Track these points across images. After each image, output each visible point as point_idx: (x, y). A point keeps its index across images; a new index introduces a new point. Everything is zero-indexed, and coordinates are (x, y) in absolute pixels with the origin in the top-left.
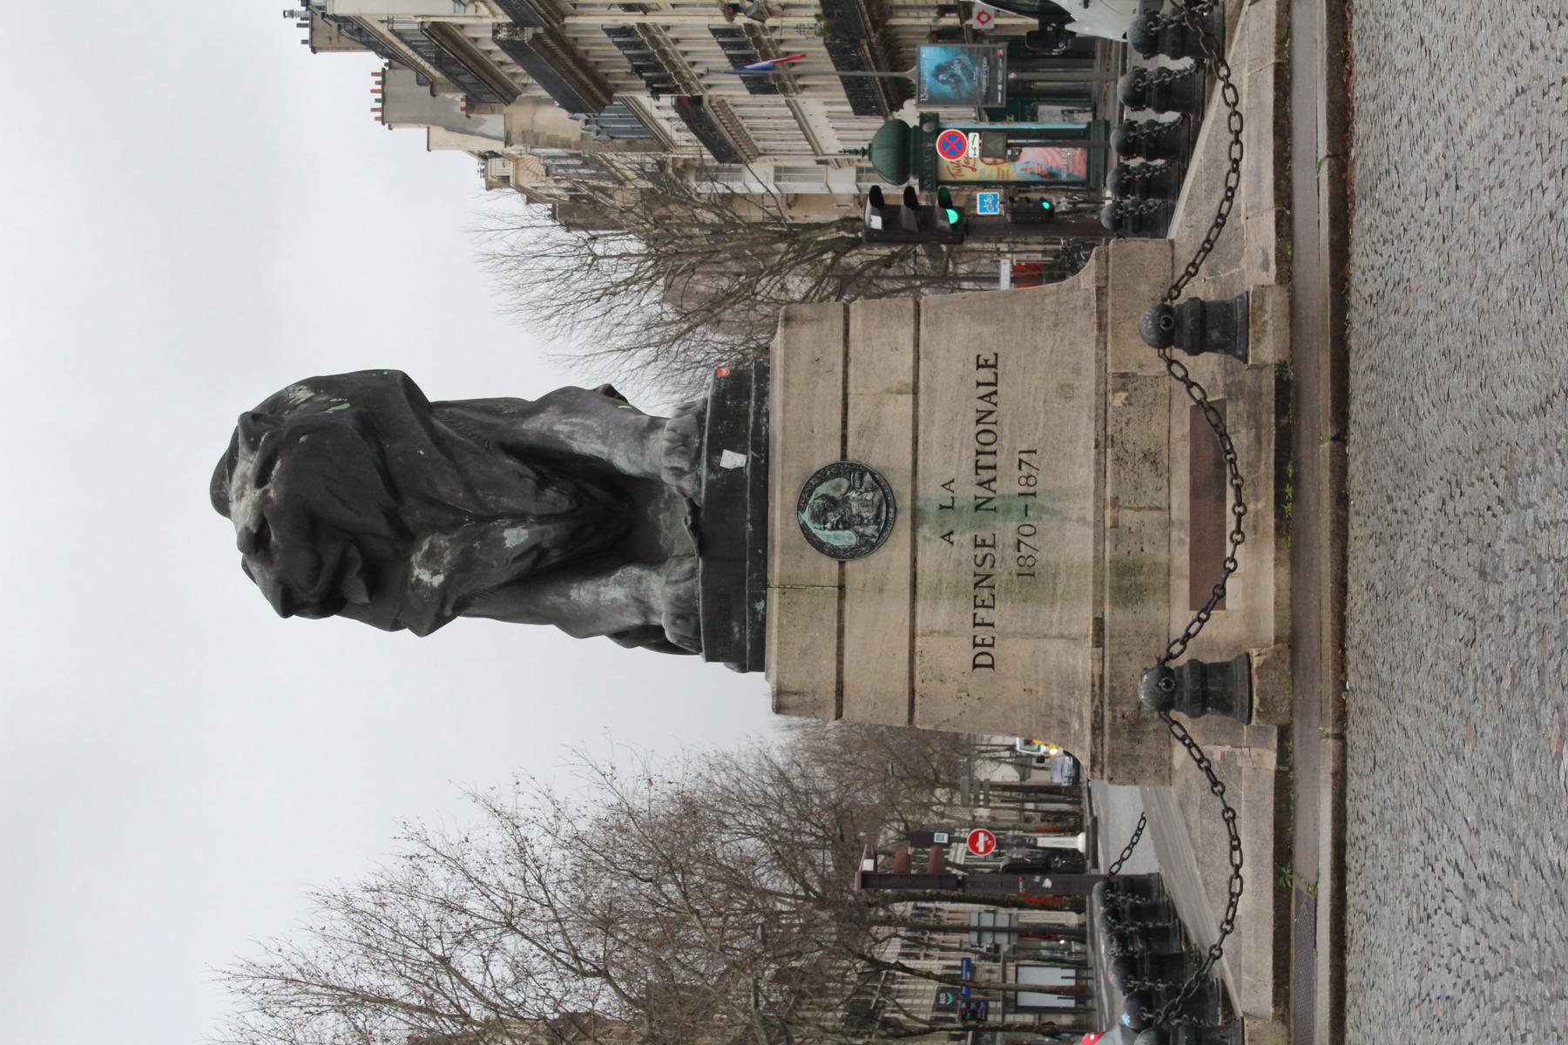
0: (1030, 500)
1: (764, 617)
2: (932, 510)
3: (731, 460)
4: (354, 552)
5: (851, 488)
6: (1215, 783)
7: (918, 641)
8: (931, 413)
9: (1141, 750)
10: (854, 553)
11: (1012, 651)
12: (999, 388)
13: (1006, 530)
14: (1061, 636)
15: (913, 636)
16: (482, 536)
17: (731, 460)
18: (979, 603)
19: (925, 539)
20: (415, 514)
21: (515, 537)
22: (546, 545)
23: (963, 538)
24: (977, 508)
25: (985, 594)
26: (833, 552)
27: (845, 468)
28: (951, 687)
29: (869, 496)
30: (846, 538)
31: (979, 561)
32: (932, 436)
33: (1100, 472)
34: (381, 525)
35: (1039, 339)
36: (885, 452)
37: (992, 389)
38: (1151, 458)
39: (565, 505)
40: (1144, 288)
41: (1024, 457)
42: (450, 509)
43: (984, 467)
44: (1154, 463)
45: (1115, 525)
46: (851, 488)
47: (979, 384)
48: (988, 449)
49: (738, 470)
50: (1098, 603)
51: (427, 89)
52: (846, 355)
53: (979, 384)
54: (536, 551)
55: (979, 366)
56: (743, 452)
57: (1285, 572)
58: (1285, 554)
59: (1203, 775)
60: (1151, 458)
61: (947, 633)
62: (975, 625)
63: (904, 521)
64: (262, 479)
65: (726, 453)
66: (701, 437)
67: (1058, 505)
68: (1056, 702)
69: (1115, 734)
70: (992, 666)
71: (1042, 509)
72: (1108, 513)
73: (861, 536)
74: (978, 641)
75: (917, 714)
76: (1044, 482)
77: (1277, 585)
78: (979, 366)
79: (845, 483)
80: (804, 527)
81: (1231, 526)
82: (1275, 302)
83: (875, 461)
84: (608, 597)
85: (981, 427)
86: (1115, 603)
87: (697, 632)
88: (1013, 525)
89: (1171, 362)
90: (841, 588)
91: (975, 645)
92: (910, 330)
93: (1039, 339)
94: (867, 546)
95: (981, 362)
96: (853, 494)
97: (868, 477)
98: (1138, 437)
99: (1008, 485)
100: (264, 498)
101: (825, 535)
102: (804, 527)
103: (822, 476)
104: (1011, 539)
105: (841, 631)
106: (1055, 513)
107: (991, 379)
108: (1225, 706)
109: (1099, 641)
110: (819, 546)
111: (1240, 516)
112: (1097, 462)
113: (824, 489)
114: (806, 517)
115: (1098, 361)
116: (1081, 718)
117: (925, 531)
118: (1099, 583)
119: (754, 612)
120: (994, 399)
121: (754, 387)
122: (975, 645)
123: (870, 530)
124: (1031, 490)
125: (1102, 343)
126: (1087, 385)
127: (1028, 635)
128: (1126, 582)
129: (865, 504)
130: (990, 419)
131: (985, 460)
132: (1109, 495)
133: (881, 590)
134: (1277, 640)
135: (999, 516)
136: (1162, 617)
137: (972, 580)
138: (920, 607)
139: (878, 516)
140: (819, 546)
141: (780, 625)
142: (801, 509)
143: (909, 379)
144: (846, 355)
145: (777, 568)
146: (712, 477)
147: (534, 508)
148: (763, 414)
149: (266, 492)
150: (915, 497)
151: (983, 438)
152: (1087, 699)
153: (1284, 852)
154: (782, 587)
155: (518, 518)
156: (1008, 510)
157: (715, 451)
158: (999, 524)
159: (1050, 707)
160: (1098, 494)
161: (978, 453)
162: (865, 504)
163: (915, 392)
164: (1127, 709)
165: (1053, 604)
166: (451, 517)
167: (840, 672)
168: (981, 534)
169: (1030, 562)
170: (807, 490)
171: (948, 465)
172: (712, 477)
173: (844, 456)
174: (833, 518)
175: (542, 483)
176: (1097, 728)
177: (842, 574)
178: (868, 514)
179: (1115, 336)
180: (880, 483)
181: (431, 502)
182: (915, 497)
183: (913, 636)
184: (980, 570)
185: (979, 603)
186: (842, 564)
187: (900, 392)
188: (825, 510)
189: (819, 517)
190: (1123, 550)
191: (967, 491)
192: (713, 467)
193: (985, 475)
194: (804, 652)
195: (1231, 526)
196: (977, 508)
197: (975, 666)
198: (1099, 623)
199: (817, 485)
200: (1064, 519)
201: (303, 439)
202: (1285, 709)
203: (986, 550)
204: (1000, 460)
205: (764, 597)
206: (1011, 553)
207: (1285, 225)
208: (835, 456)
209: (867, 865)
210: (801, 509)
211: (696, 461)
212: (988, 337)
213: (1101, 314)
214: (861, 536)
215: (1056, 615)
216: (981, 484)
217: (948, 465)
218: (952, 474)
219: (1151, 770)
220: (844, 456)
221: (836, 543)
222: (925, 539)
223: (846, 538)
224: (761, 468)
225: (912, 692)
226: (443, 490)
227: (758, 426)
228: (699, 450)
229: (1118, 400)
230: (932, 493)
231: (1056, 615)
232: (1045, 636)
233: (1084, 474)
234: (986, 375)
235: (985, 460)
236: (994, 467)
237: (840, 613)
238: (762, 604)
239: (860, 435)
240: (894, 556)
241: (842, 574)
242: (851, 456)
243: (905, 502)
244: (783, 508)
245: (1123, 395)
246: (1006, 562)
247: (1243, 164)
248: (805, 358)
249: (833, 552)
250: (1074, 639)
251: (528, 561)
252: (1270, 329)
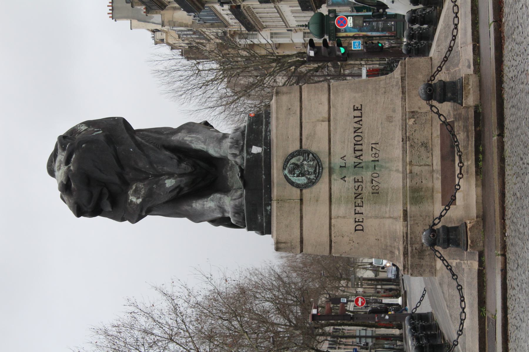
0: (376, 163)
1: (271, 212)
2: (337, 168)
3: (256, 150)
4: (105, 191)
5: (304, 160)
6: (454, 275)
7: (333, 221)
8: (336, 129)
9: (423, 262)
11: (370, 224)
12: (363, 118)
13: (367, 175)
14: (390, 217)
15: (330, 219)
16: (157, 183)
17: (256, 150)
18: (357, 205)
19: (335, 180)
20: (130, 175)
21: (170, 183)
22: (182, 186)
23: (350, 179)
24: (355, 167)
25: (359, 201)
26: (298, 186)
27: (301, 152)
28: (346, 239)
29: (311, 163)
30: (302, 180)
31: (356, 188)
32: (336, 138)
33: (404, 151)
34: (116, 180)
35: (379, 98)
36: (318, 145)
37: (360, 119)
38: (424, 145)
39: (189, 169)
40: (420, 77)
41: (374, 146)
42: (145, 172)
43: (357, 150)
44: (426, 147)
45: (411, 172)
46: (304, 160)
47: (355, 117)
48: (359, 143)
49: (259, 154)
50: (405, 204)
51: (130, 5)
52: (301, 107)
53: (355, 117)
54: (178, 188)
55: (354, 110)
56: (261, 146)
57: (480, 189)
58: (480, 182)
59: (449, 272)
60: (424, 145)
61: (344, 217)
62: (355, 214)
63: (326, 173)
64: (67, 162)
65: (254, 147)
66: (244, 141)
67: (388, 165)
68: (389, 244)
69: (413, 256)
70: (362, 230)
71: (381, 167)
72: (408, 167)
73: (309, 179)
74: (357, 220)
75: (333, 250)
76: (382, 156)
77: (477, 195)
78: (354, 110)
79: (302, 158)
80: (286, 176)
81: (457, 171)
82: (473, 81)
83: (314, 149)
84: (208, 206)
85: (356, 134)
86: (411, 204)
87: (244, 219)
88: (370, 173)
89: (432, 106)
90: (301, 200)
91: (356, 222)
92: (326, 96)
93: (379, 98)
94: (311, 183)
95: (355, 108)
96: (305, 162)
97: (311, 155)
98: (420, 136)
99: (368, 157)
100: (69, 170)
101: (294, 179)
102: (286, 176)
103: (292, 155)
104: (369, 179)
105: (301, 218)
106: (386, 168)
107: (360, 115)
108: (457, 244)
109: (405, 219)
110: (292, 183)
111: (461, 167)
112: (403, 147)
113: (293, 161)
114: (286, 172)
115: (402, 107)
116: (399, 249)
117: (334, 176)
118: (405, 196)
119: (266, 210)
120: (361, 123)
121: (264, 120)
122: (356, 222)
123: (312, 177)
124: (377, 159)
125: (404, 99)
126: (398, 116)
127: (376, 217)
128: (416, 195)
129: (310, 166)
130: (360, 131)
131: (358, 147)
132: (408, 160)
133: (317, 201)
134: (477, 217)
135: (364, 170)
136: (431, 209)
137: (354, 196)
138: (333, 207)
139: (315, 171)
140: (292, 183)
141: (277, 216)
142: (284, 169)
143: (326, 116)
144: (301, 107)
145: (275, 193)
146: (248, 157)
147: (178, 171)
148: (268, 131)
149: (69, 167)
150: (330, 163)
151: (357, 139)
152: (401, 243)
153: (482, 302)
154: (278, 200)
155: (171, 175)
156: (367, 167)
157: (249, 146)
158: (364, 173)
159: (386, 246)
160: (404, 160)
161: (355, 145)
162: (310, 166)
163: (329, 121)
164: (417, 246)
165: (386, 205)
166: (144, 175)
167: (301, 234)
168: (357, 177)
169: (377, 188)
170: (287, 161)
171: (343, 150)
172: (248, 157)
173: (301, 147)
174: (297, 172)
175: (180, 161)
176: (405, 254)
177: (301, 195)
178: (311, 170)
179: (409, 96)
180: (316, 158)
181: (136, 169)
182: (330, 163)
183: (330, 219)
184: (356, 192)
185: (357, 205)
186: (301, 190)
187: (323, 121)
188: (294, 169)
189: (292, 172)
190: (414, 182)
191: (351, 160)
192: (249, 153)
193: (358, 153)
194: (287, 226)
195: (457, 171)
196: (355, 167)
197: (356, 230)
198: (405, 212)
199: (291, 159)
200: (390, 170)
201: (83, 146)
202: (481, 244)
203: (359, 184)
204: (364, 147)
205: (271, 205)
206: (369, 184)
207: (476, 50)
208: (297, 147)
209: (314, 311)
210: (284, 169)
211: (242, 150)
212: (357, 98)
213: (403, 87)
214: (309, 179)
215: (388, 209)
216: (356, 157)
217: (343, 150)
218: (345, 154)
219: (428, 270)
220: (301, 147)
221: (299, 182)
222: (335, 180)
223: (302, 180)
224: (268, 153)
225: (331, 241)
226: (141, 165)
227: (266, 136)
228: (243, 146)
229: (411, 122)
230: (337, 161)
231: (388, 209)
232: (384, 218)
233: (398, 152)
234: (357, 113)
235: (358, 147)
236: (362, 150)
237: (301, 210)
238: (270, 207)
239: (307, 139)
240: (322, 186)
241: (301, 195)
242: (304, 147)
243: (326, 165)
244: (277, 169)
245: (413, 120)
246: (367, 189)
247: (459, 26)
248: (285, 108)
249: (298, 186)
250: (395, 219)
251: (175, 192)
252: (471, 92)
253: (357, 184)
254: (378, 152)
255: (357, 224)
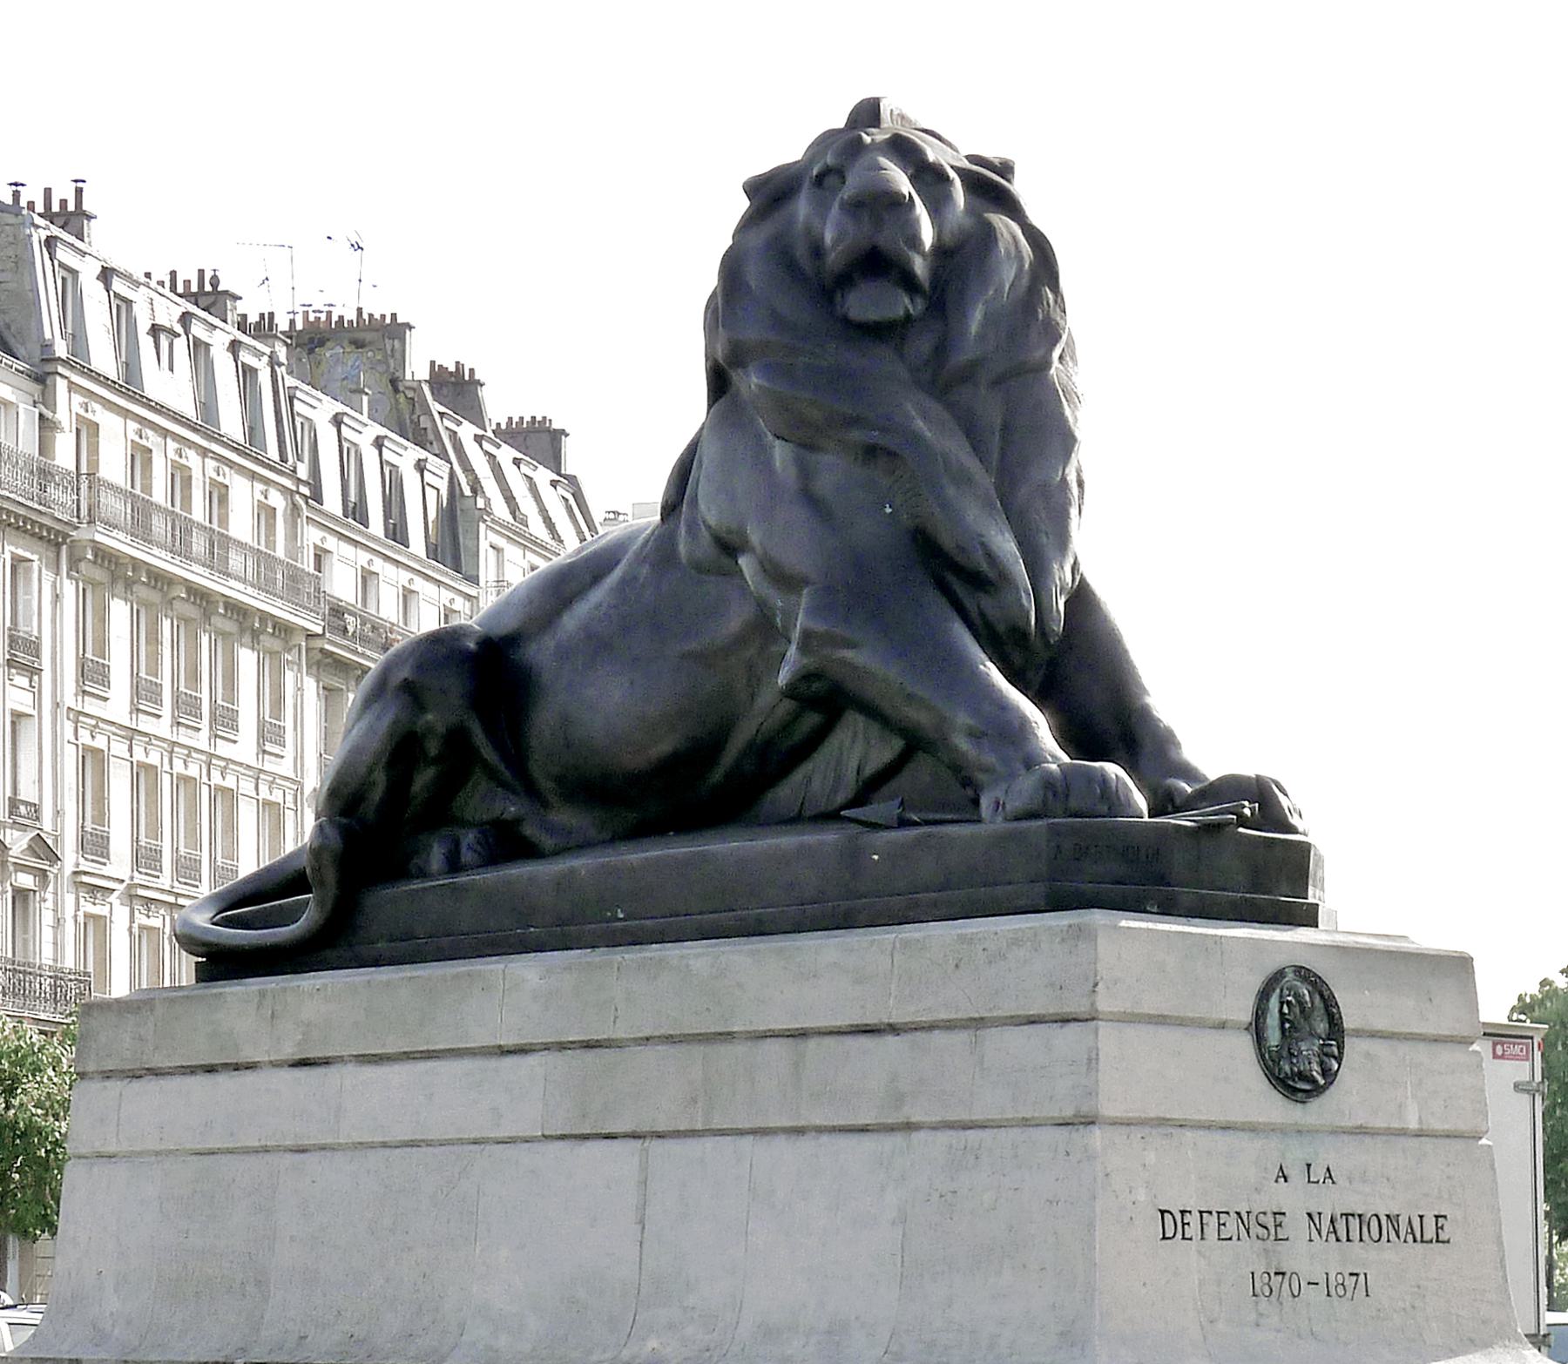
10: (1260, 1039)
12: (1419, 1246)
25: (1232, 1225)
36: (1355, 1091)
41: (1362, 1277)
48: (1365, 1229)
53: (1421, 1217)
70: (1164, 1238)
74: (1187, 1218)
85: (1384, 1220)
91: (1183, 1212)
101: (1274, 1003)
102: (1279, 975)
107: (1427, 1237)
110: (1264, 995)
120: (1410, 1238)
122: (1183, 1212)
151: (1374, 1223)
177: (1236, 1026)
184: (1253, 1217)
193: (1341, 1226)
197: (1162, 1212)
234: (1430, 1233)
239: (1368, 1055)
251: (985, 567)
253: (1269, 1221)
254: (1349, 1294)
255: (1178, 1217)
